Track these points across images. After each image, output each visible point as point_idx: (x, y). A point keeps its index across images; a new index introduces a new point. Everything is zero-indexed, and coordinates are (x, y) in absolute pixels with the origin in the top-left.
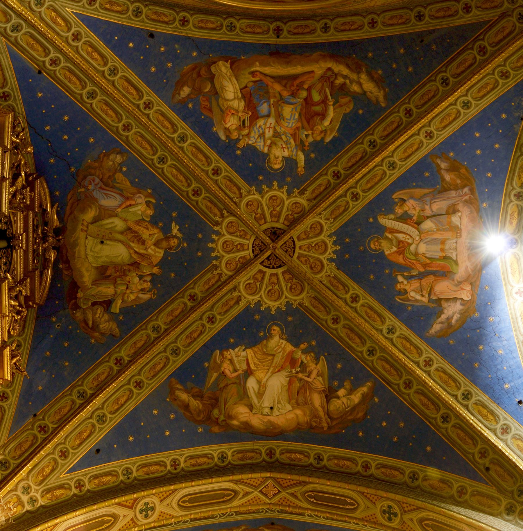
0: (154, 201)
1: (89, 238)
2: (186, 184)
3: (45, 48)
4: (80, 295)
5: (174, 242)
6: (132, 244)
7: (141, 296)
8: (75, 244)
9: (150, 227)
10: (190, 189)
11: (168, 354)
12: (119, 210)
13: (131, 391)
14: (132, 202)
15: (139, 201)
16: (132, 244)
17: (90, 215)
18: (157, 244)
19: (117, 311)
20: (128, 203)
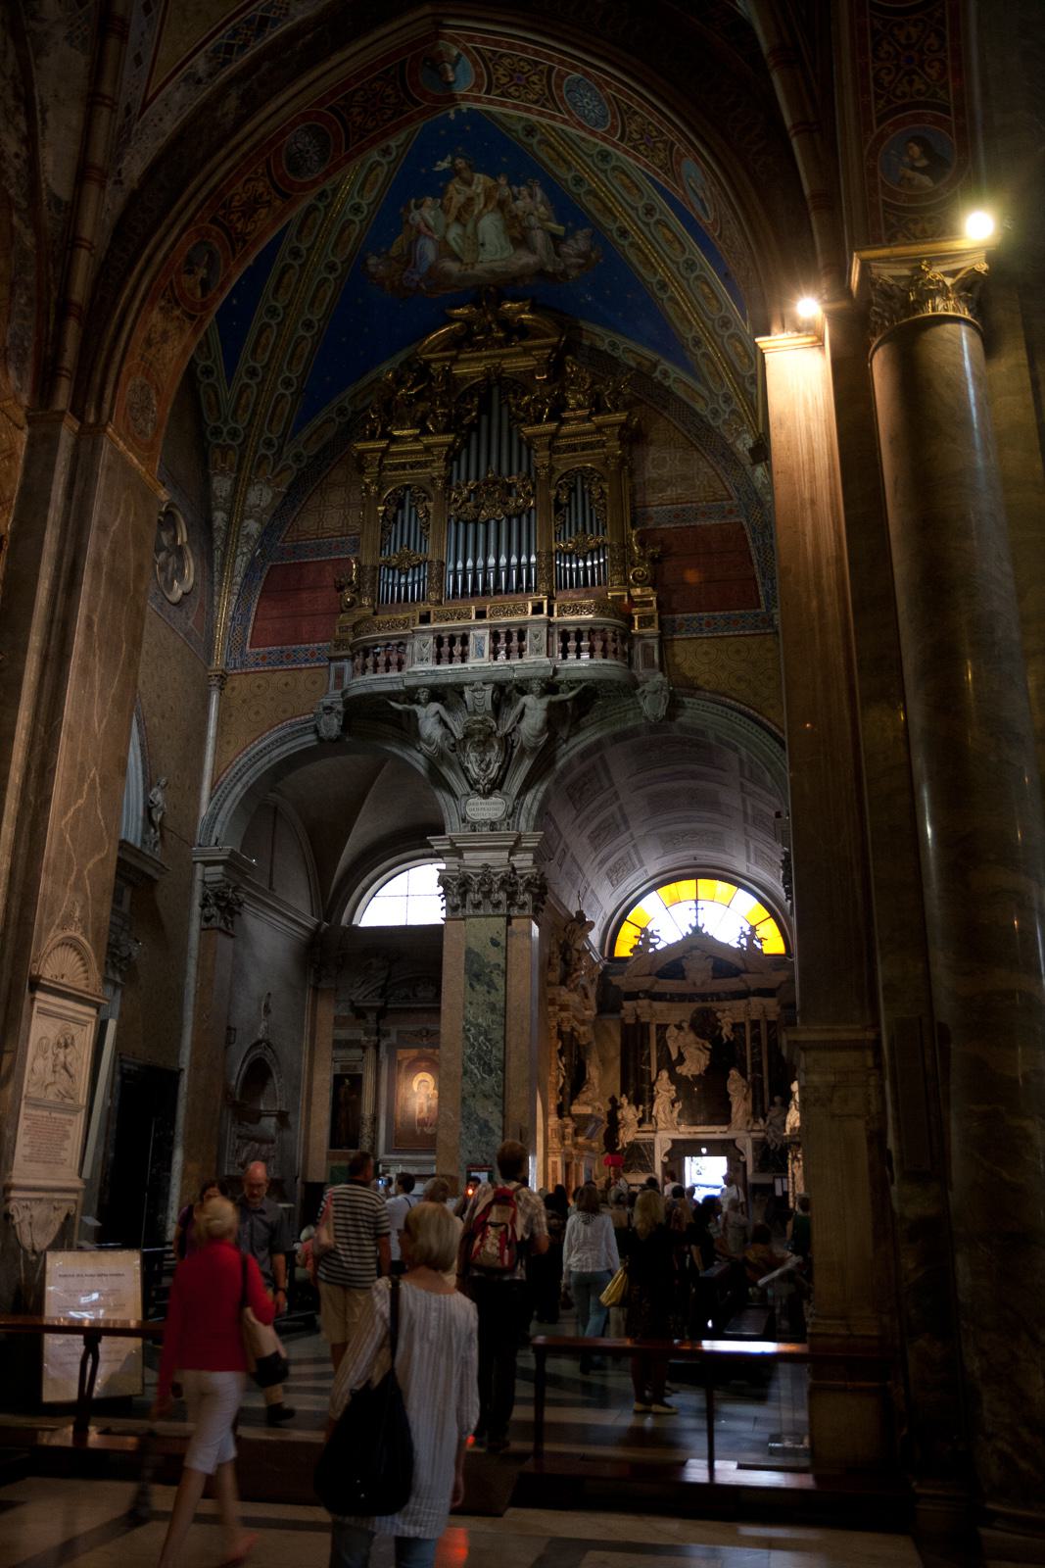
0: (413, 201)
1: (480, 259)
2: (379, 168)
3: (277, 402)
4: (550, 268)
5: (460, 163)
6: (476, 212)
7: (538, 199)
8: (492, 272)
9: (449, 196)
10: (384, 161)
11: (608, 167)
12: (436, 237)
13: (658, 222)
14: (422, 225)
15: (418, 218)
16: (476, 212)
17: (452, 267)
18: (468, 183)
19: (562, 228)
20: (425, 230)
